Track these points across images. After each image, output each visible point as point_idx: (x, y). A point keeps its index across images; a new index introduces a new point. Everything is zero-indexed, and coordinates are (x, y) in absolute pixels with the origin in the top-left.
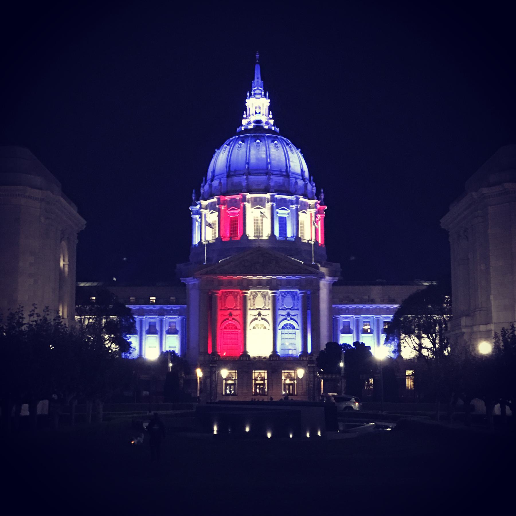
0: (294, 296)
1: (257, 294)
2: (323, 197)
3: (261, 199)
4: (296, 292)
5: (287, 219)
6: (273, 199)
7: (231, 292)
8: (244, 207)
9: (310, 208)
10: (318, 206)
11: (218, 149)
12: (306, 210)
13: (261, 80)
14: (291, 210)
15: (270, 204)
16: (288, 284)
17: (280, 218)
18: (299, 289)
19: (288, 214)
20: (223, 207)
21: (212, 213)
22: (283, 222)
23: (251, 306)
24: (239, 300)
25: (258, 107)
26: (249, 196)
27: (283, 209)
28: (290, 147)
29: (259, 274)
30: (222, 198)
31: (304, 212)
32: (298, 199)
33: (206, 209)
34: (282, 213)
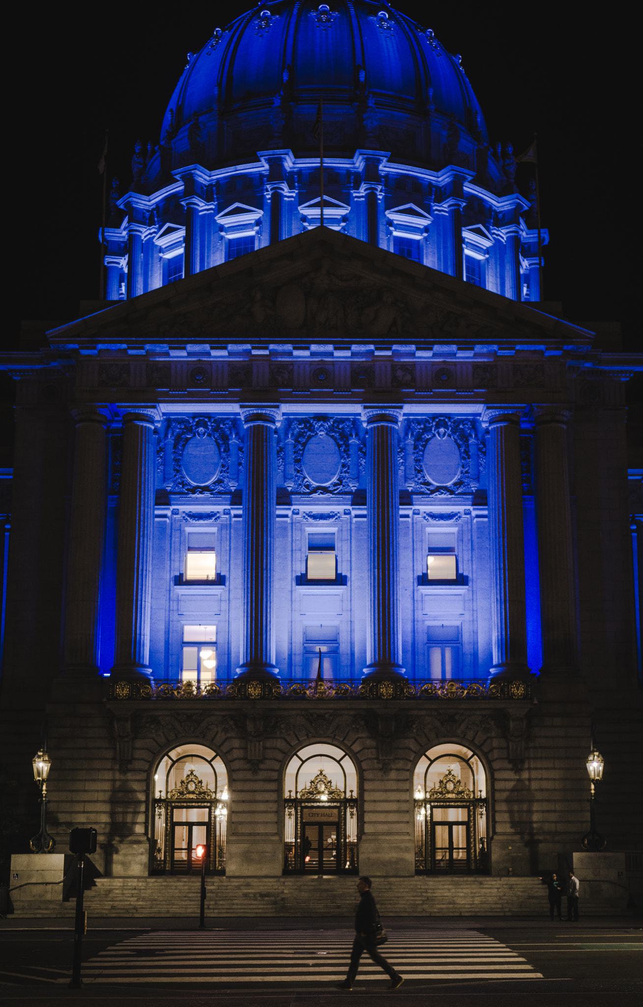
0: (465, 437)
1: (311, 428)
4: (473, 421)
5: (423, 243)
6: (371, 173)
7: (202, 419)
8: (277, 197)
11: (197, 47)
12: (489, 231)
14: (437, 219)
15: (362, 191)
16: (443, 382)
18: (488, 402)
19: (426, 229)
20: (202, 206)
21: (170, 231)
23: (286, 478)
24: (233, 450)
27: (410, 212)
29: (323, 336)
30: (203, 177)
31: (478, 232)
33: (150, 223)
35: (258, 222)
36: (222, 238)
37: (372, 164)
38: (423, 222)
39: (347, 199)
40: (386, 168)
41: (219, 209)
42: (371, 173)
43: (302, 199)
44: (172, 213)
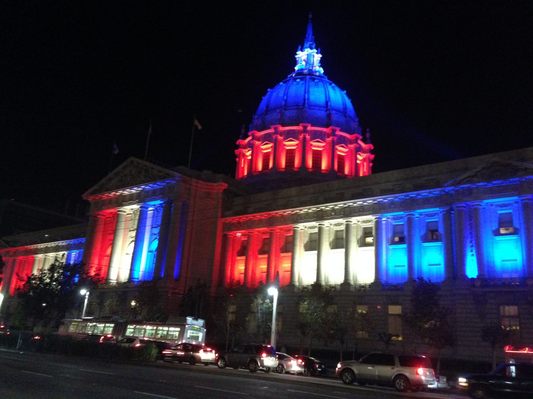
2: (368, 135)
3: (293, 131)
9: (351, 143)
10: (360, 142)
12: (347, 145)
13: (313, 35)
17: (314, 151)
19: (324, 147)
21: (249, 150)
22: (317, 156)
25: (308, 57)
26: (282, 129)
28: (333, 87)
31: (342, 147)
32: (334, 131)
34: (317, 145)
35: (272, 147)
36: (262, 152)
37: (305, 127)
38: (324, 144)
39: (297, 139)
40: (309, 128)
41: (263, 142)
42: (305, 131)
43: (285, 139)
44: (250, 146)
